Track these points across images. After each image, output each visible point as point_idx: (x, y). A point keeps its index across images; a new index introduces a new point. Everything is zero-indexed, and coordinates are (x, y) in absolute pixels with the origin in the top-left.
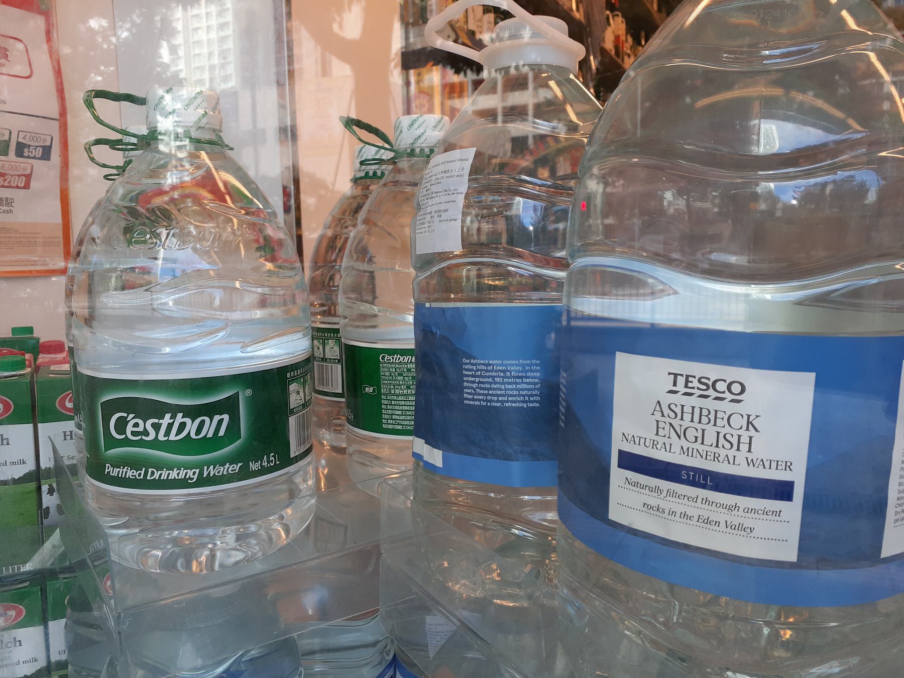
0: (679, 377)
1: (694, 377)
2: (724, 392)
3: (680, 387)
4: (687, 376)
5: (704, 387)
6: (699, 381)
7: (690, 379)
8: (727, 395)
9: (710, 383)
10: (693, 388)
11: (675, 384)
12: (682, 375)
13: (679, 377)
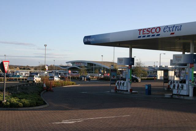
0: (141, 30)
1: (145, 29)
2: (154, 33)
3: (142, 35)
4: (144, 30)
5: (148, 32)
6: (147, 31)
7: (144, 30)
8: (156, 34)
9: (150, 30)
10: (145, 34)
11: (140, 34)
12: (142, 30)
13: (141, 30)
